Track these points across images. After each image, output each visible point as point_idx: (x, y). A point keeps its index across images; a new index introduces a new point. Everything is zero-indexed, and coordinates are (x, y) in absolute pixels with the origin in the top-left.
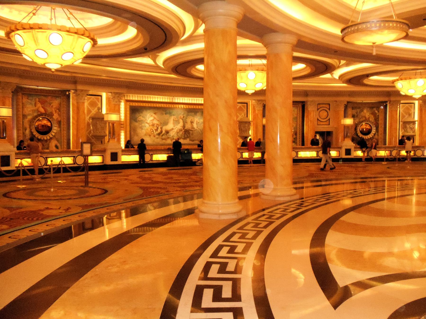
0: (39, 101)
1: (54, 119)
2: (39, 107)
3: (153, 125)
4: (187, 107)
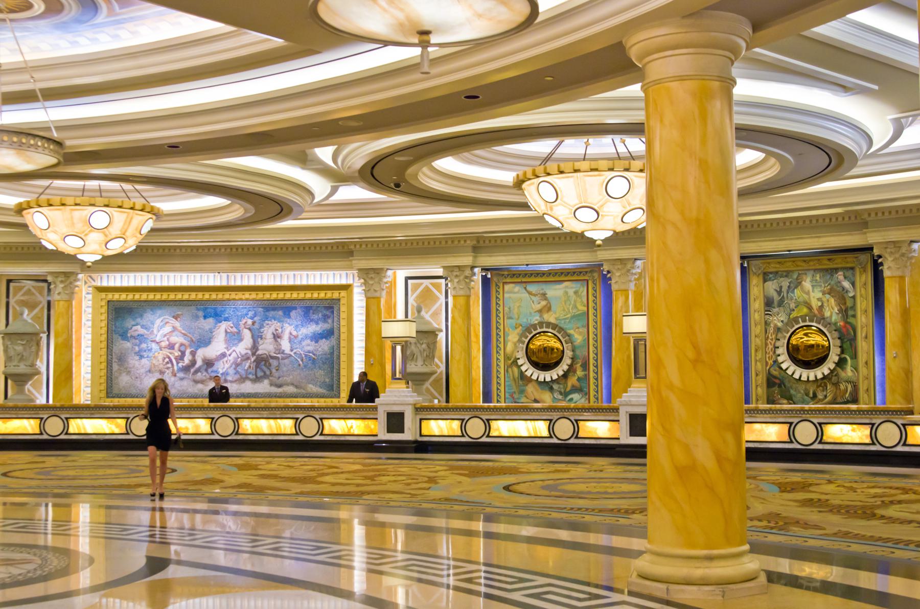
3: (171, 346)
4: (260, 295)
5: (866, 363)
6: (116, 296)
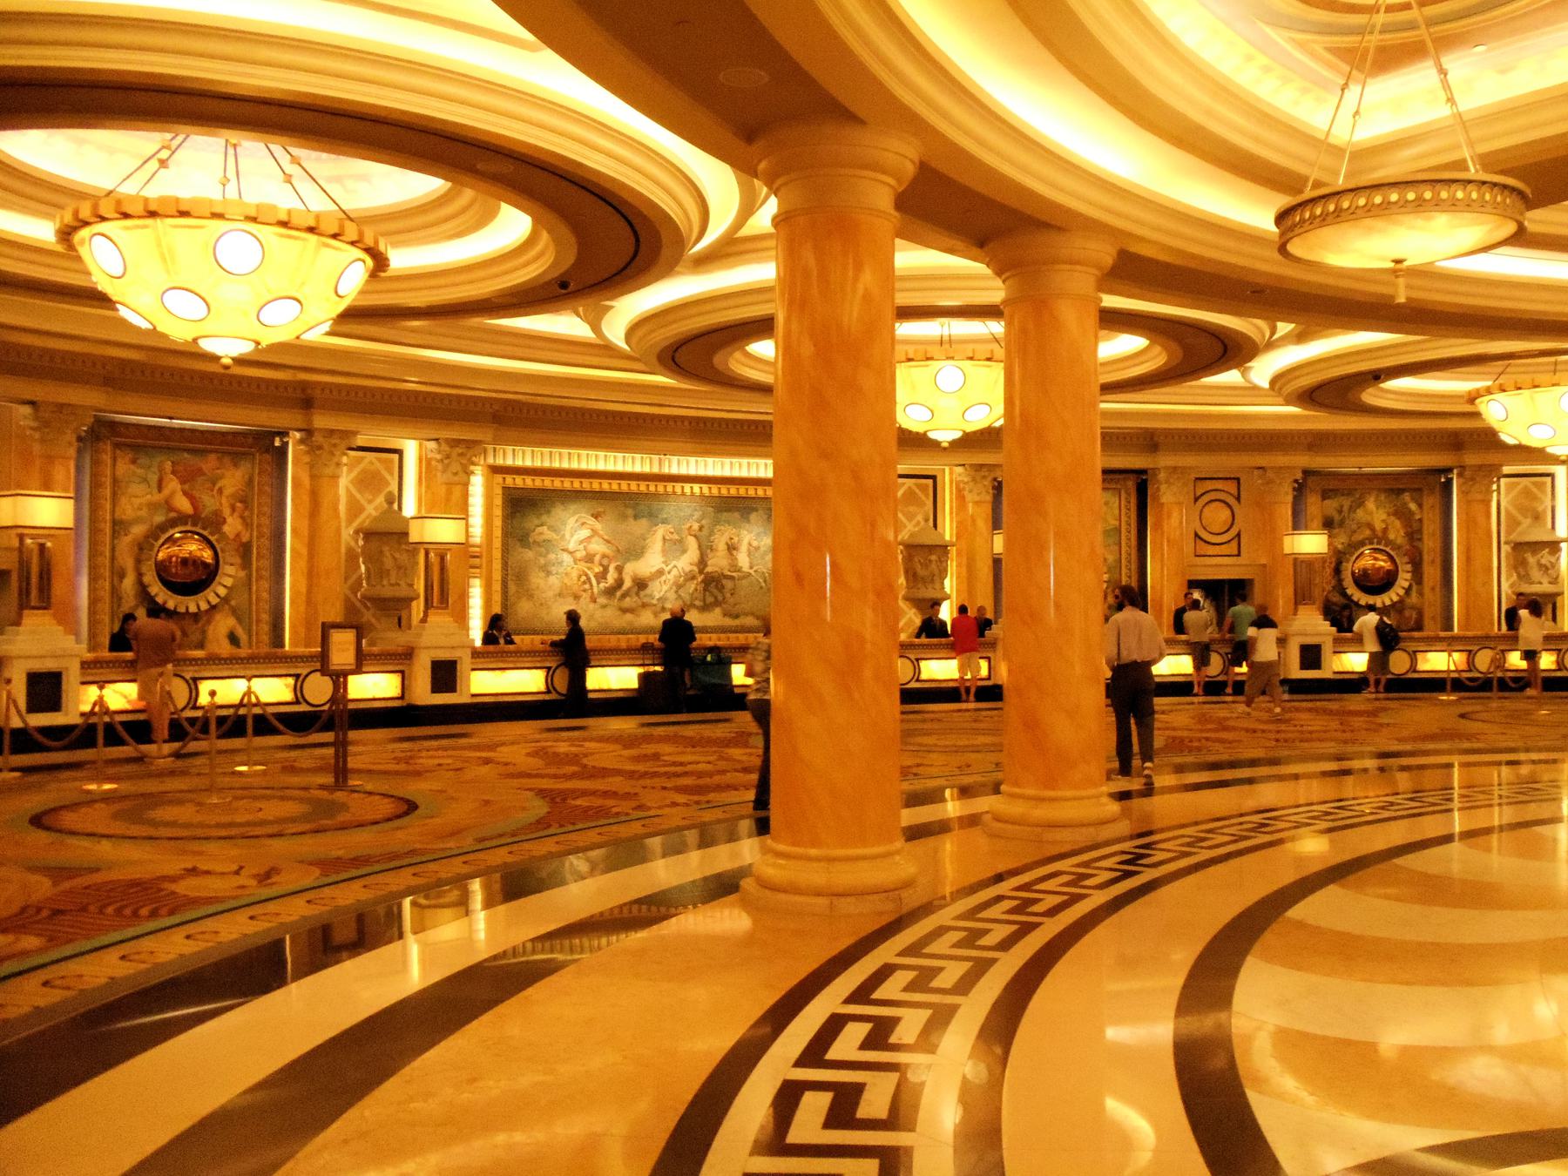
0: (173, 472)
1: (223, 536)
2: (173, 493)
3: (589, 558)
5: (1433, 589)
6: (519, 481)
